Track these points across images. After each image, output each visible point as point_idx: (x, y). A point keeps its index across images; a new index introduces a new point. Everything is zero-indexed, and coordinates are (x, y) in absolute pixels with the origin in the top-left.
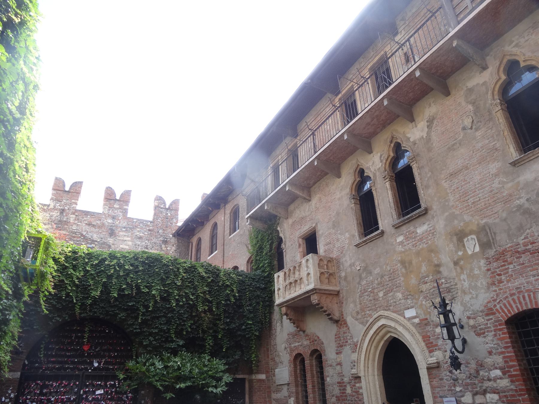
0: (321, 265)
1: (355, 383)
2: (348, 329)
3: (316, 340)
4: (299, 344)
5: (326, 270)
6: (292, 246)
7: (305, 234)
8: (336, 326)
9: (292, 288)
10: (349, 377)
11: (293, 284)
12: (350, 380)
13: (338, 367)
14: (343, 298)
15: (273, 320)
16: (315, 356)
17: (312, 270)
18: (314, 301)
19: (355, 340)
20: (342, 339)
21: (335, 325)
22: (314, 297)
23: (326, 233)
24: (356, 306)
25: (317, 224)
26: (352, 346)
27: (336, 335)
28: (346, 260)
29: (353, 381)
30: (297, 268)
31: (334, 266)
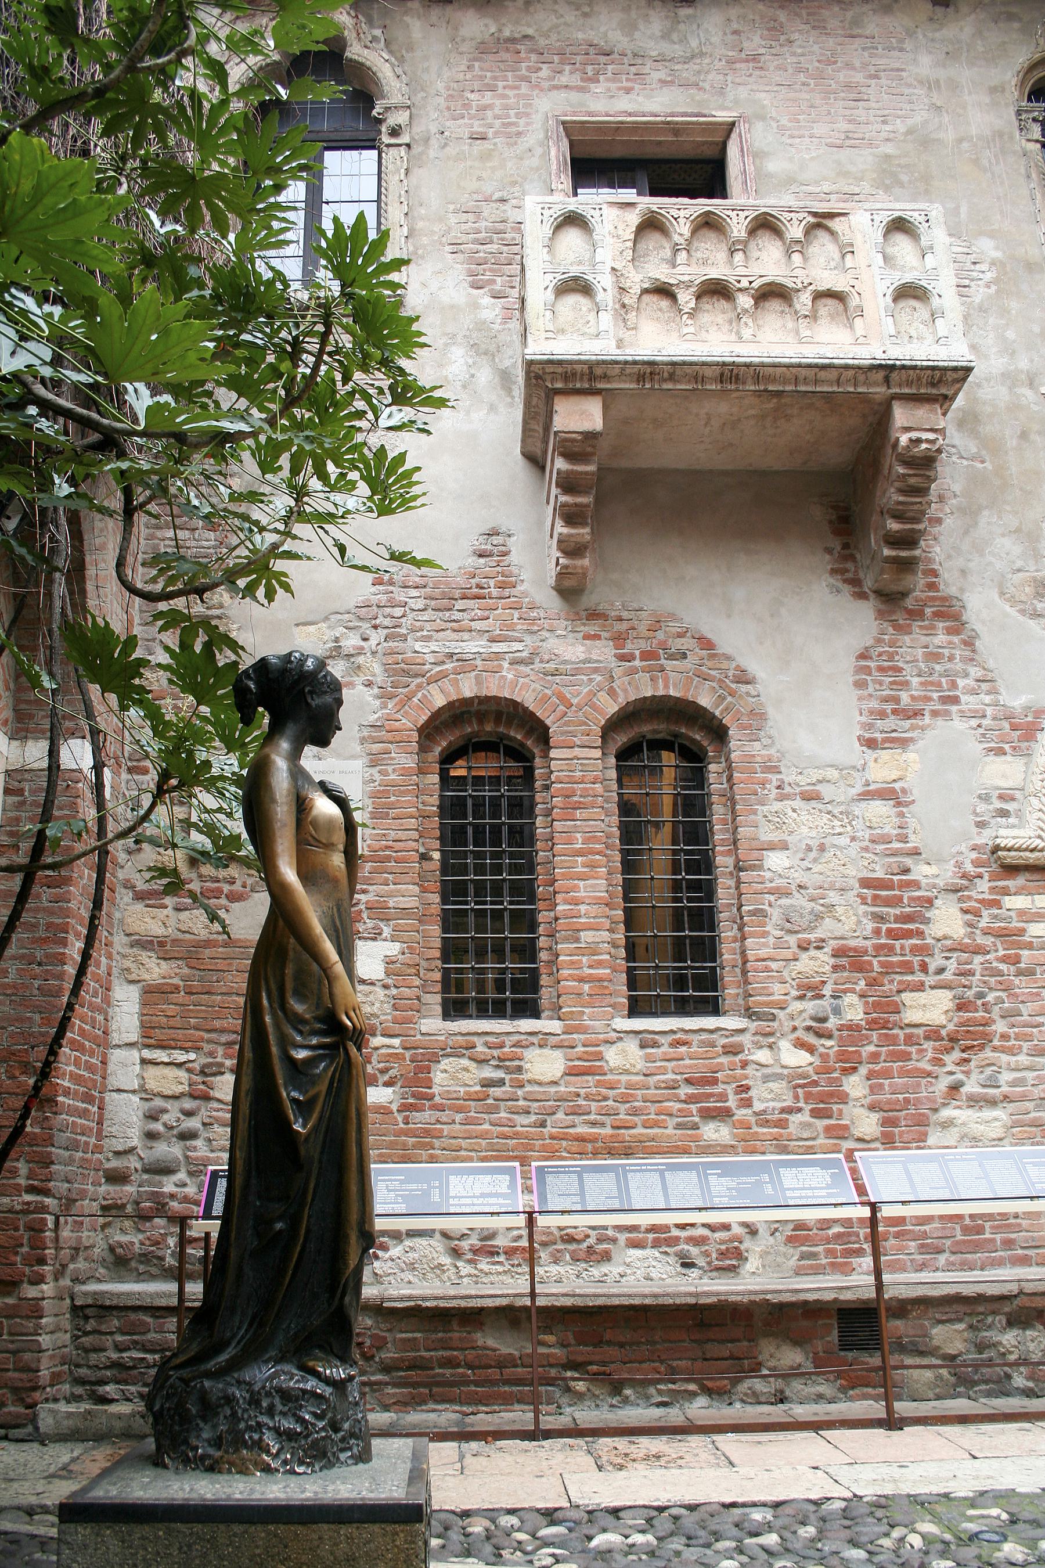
1: (1005, 891)
2: (969, 644)
3: (684, 656)
6: (486, 145)
7: (619, 128)
9: (705, 318)
10: (959, 865)
12: (964, 876)
13: (879, 810)
16: (621, 739)
19: (1017, 702)
20: (915, 681)
23: (817, 183)
26: (985, 722)
27: (863, 656)
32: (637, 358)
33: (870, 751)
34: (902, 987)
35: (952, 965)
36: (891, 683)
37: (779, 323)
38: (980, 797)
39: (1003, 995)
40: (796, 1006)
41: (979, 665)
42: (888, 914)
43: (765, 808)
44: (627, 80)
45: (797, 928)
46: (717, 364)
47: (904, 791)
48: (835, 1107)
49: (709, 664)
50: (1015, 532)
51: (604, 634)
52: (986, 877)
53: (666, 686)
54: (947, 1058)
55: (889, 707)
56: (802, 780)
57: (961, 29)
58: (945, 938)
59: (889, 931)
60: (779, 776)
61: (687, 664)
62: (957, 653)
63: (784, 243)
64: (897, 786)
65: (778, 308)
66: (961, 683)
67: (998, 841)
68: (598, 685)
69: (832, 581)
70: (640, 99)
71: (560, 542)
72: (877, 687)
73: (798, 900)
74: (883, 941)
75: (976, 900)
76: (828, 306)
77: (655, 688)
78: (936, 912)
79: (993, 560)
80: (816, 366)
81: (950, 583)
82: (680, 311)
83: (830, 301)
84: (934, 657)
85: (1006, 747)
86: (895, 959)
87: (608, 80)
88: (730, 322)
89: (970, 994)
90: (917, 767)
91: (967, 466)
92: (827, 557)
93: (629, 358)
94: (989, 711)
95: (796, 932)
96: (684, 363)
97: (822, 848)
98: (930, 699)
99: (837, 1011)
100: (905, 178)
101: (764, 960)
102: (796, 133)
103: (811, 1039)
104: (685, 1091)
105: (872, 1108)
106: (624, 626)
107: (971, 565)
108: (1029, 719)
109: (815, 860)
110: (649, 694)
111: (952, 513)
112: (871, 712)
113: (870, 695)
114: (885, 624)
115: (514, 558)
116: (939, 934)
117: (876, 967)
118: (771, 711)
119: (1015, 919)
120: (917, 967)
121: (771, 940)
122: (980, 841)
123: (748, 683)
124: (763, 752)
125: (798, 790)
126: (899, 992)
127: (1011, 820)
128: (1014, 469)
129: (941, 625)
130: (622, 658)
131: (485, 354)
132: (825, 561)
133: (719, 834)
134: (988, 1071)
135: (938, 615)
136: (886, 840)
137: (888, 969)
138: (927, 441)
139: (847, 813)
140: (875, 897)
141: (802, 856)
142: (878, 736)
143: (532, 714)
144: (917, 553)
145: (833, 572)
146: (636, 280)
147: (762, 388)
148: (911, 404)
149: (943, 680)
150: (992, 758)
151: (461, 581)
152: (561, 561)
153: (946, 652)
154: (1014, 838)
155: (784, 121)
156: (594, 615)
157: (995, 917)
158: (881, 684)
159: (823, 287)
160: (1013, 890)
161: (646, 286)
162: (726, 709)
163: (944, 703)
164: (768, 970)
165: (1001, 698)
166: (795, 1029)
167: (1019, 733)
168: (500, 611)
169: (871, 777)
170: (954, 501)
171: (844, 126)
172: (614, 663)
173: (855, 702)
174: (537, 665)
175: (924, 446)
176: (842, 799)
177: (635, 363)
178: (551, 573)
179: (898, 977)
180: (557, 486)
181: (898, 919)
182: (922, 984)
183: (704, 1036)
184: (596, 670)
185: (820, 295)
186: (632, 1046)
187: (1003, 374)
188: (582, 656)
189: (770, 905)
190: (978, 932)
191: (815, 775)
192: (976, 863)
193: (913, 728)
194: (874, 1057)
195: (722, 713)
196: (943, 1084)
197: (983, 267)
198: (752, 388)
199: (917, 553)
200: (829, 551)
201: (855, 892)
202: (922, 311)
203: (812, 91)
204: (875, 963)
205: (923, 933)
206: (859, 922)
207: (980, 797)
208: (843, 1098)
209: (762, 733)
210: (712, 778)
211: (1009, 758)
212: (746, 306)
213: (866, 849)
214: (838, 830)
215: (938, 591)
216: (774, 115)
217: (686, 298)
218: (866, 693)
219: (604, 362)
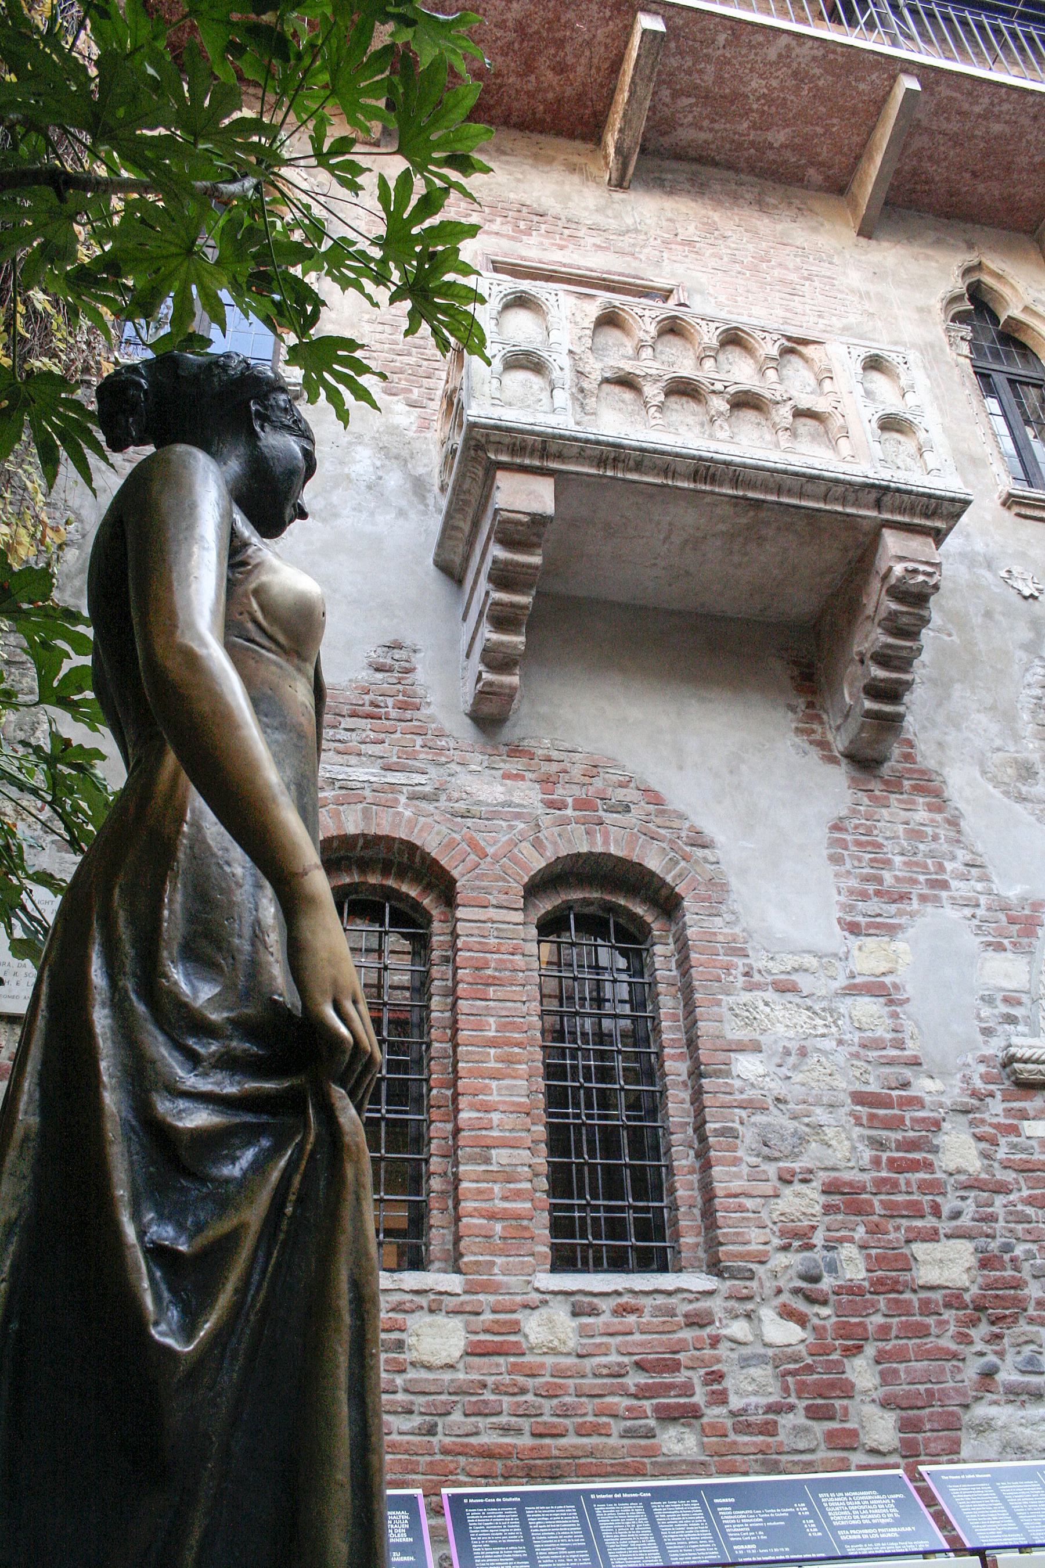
1: (1024, 1115)
2: (953, 823)
3: (627, 809)
4: (392, 778)
10: (966, 1079)
12: (974, 1094)
13: (867, 1007)
16: (545, 905)
19: (1013, 892)
20: (898, 860)
24: (1017, 738)
26: (980, 912)
27: (836, 827)
29: (996, 1107)
33: (852, 937)
34: (911, 1236)
35: (969, 1208)
36: (872, 860)
37: (755, 434)
38: (982, 998)
39: (1034, 1247)
40: (781, 1260)
42: (887, 1139)
43: (731, 999)
45: (777, 1154)
46: (693, 458)
47: (896, 986)
48: (838, 1403)
49: (659, 821)
50: (990, 709)
51: (529, 775)
52: (999, 1096)
53: (606, 842)
54: (975, 1333)
55: (871, 888)
56: (775, 967)
57: (884, 258)
58: (959, 1172)
59: (891, 1161)
60: (746, 961)
61: (630, 819)
62: (942, 833)
63: (756, 362)
64: (888, 980)
65: (753, 419)
66: (949, 866)
67: (1012, 1050)
68: (520, 833)
69: (797, 740)
71: (485, 650)
72: (856, 863)
73: (776, 1118)
74: (884, 1174)
75: (990, 1125)
76: (806, 426)
77: (593, 843)
78: (946, 1138)
79: (971, 736)
80: (804, 475)
81: (927, 755)
82: (646, 403)
83: (809, 422)
84: (916, 835)
85: (1006, 942)
86: (899, 1198)
87: (541, 235)
88: (702, 425)
89: (994, 1245)
90: (908, 959)
91: (934, 637)
92: (790, 715)
93: (592, 437)
94: (983, 900)
95: (776, 1159)
96: (655, 452)
97: (803, 1053)
98: (915, 882)
99: (832, 1268)
101: (736, 1196)
103: (800, 1305)
104: (635, 1380)
105: (886, 1404)
106: (554, 767)
107: (949, 738)
108: (1027, 912)
109: (795, 1067)
110: (584, 849)
111: (923, 683)
112: (851, 892)
113: (848, 872)
114: (860, 794)
115: (420, 676)
116: (952, 1167)
117: (878, 1208)
118: (734, 883)
119: (1037, 1149)
120: (927, 1210)
121: (745, 1169)
122: (988, 1051)
123: (704, 847)
124: (726, 930)
125: (770, 979)
126: (908, 1241)
127: (1021, 1028)
128: (982, 646)
129: (921, 800)
130: (551, 805)
131: (396, 458)
132: (788, 721)
133: (670, 1032)
134: (1027, 1350)
135: (918, 789)
136: (878, 1044)
137: (893, 1212)
138: (925, 573)
139: (831, 1011)
140: (872, 1117)
141: (779, 1061)
142: (860, 919)
143: (435, 862)
144: (901, 709)
145: (798, 731)
146: (596, 368)
147: (741, 493)
148: (903, 535)
149: (929, 861)
150: (990, 954)
151: (351, 696)
152: (484, 675)
153: (929, 830)
154: (1030, 1047)
155: (722, 298)
156: (515, 751)
157: (1014, 1146)
158: (860, 860)
160: (1032, 1113)
161: (607, 375)
162: (680, 875)
163: (932, 887)
164: (742, 1209)
165: (994, 886)
166: (779, 1291)
167: (1018, 927)
168: (398, 735)
169: (857, 969)
171: (781, 313)
172: (540, 809)
173: (832, 879)
174: (443, 803)
175: (921, 578)
176: (823, 992)
177: (598, 443)
178: (467, 693)
179: (905, 1222)
180: (490, 579)
181: (901, 1146)
182: (936, 1231)
183: (661, 1300)
184: (518, 816)
185: (799, 413)
186: (560, 1313)
187: (960, 554)
188: (501, 798)
189: (742, 1123)
190: (996, 1165)
191: (791, 961)
192: (987, 1079)
193: (900, 913)
194: (883, 1333)
195: (674, 879)
196: (971, 1371)
198: (730, 492)
199: (901, 709)
200: (792, 709)
201: (846, 1109)
202: (908, 445)
203: (748, 279)
204: (876, 1204)
205: (931, 1165)
206: (854, 1148)
207: (982, 998)
208: (847, 1390)
209: (724, 907)
210: (658, 962)
211: (1009, 955)
212: (722, 409)
213: (856, 1056)
214: (821, 1030)
215: (915, 763)
216: (712, 292)
217: (653, 392)
218: (843, 869)
219: (561, 437)
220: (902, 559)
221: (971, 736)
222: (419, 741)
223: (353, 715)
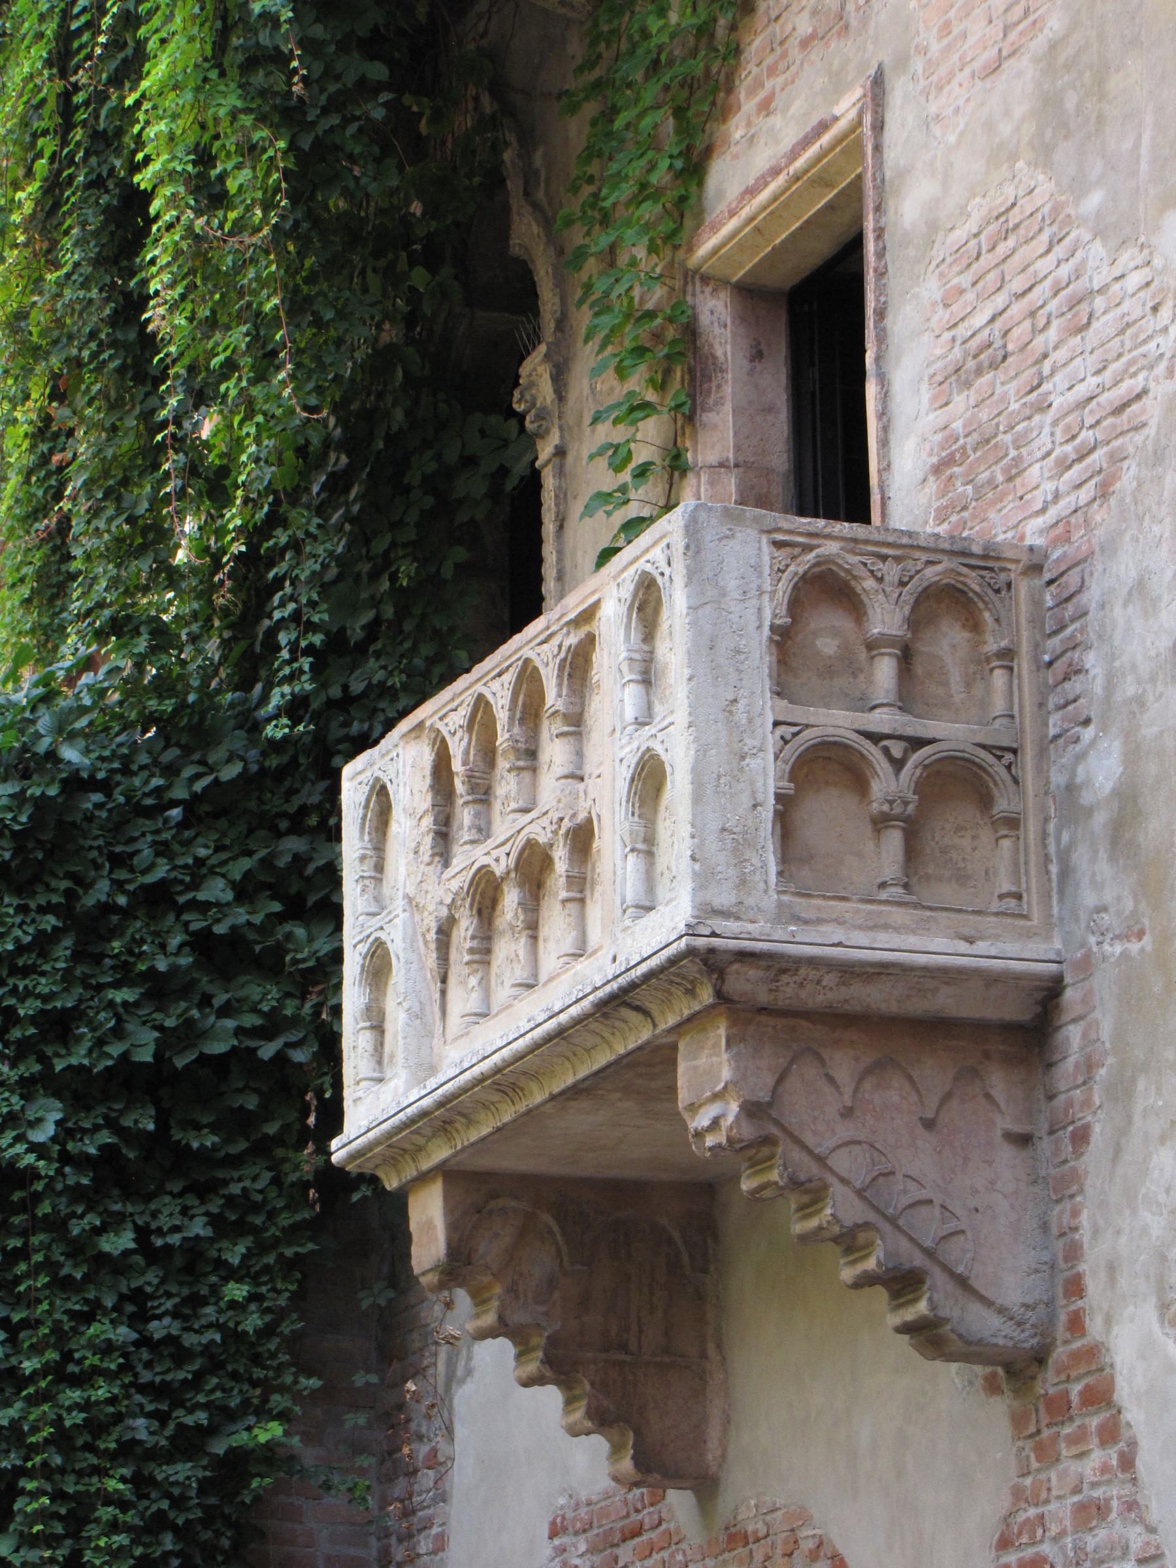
0: (828, 646)
2: (1127, 1462)
5: (883, 720)
8: (1003, 1427)
11: (511, 898)
14: (1089, 1066)
15: (415, 1340)
17: (681, 716)
18: (702, 1120)
21: (999, 1408)
22: (702, 1061)
23: (964, 213)
25: (878, 86)
28: (1140, 587)
30: (553, 696)
31: (1007, 655)
32: (409, 1111)
41: (1141, 1520)
44: (772, 71)
70: (777, 120)
100: (1071, 101)
102: (943, 71)
114: (1029, 1444)
129: (1094, 1422)
144: (922, 1307)
155: (935, 47)
159: (582, 816)
161: (444, 912)
170: (1103, 1072)
175: (710, 1141)
177: (412, 1121)
197: (1165, 313)
220: (693, 1108)
221: (1146, 1216)
222: (665, 1554)
223: (624, 1541)
